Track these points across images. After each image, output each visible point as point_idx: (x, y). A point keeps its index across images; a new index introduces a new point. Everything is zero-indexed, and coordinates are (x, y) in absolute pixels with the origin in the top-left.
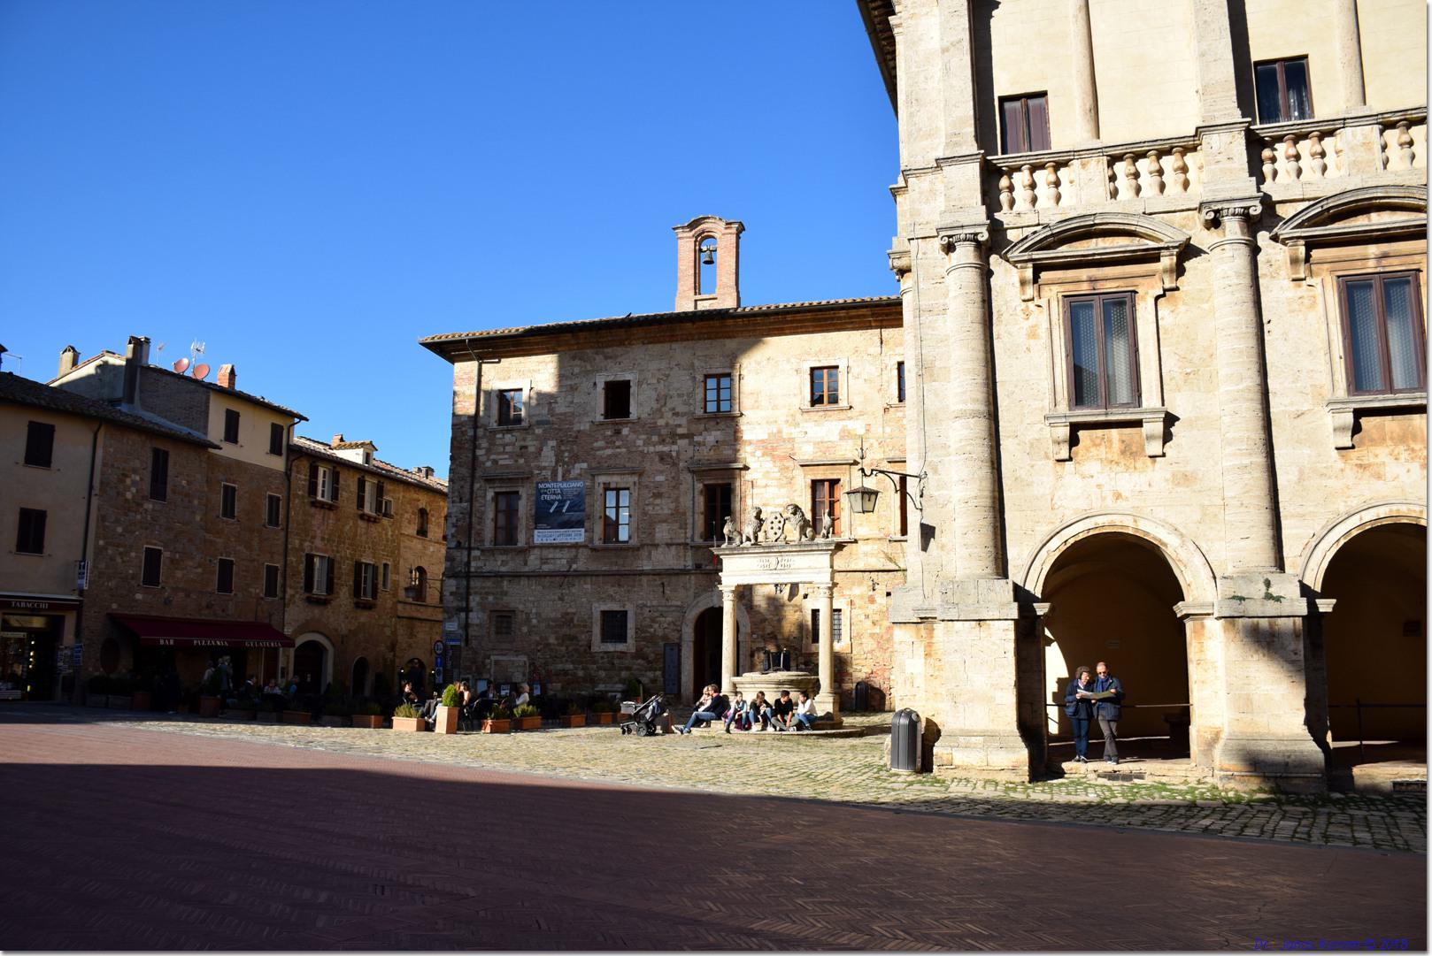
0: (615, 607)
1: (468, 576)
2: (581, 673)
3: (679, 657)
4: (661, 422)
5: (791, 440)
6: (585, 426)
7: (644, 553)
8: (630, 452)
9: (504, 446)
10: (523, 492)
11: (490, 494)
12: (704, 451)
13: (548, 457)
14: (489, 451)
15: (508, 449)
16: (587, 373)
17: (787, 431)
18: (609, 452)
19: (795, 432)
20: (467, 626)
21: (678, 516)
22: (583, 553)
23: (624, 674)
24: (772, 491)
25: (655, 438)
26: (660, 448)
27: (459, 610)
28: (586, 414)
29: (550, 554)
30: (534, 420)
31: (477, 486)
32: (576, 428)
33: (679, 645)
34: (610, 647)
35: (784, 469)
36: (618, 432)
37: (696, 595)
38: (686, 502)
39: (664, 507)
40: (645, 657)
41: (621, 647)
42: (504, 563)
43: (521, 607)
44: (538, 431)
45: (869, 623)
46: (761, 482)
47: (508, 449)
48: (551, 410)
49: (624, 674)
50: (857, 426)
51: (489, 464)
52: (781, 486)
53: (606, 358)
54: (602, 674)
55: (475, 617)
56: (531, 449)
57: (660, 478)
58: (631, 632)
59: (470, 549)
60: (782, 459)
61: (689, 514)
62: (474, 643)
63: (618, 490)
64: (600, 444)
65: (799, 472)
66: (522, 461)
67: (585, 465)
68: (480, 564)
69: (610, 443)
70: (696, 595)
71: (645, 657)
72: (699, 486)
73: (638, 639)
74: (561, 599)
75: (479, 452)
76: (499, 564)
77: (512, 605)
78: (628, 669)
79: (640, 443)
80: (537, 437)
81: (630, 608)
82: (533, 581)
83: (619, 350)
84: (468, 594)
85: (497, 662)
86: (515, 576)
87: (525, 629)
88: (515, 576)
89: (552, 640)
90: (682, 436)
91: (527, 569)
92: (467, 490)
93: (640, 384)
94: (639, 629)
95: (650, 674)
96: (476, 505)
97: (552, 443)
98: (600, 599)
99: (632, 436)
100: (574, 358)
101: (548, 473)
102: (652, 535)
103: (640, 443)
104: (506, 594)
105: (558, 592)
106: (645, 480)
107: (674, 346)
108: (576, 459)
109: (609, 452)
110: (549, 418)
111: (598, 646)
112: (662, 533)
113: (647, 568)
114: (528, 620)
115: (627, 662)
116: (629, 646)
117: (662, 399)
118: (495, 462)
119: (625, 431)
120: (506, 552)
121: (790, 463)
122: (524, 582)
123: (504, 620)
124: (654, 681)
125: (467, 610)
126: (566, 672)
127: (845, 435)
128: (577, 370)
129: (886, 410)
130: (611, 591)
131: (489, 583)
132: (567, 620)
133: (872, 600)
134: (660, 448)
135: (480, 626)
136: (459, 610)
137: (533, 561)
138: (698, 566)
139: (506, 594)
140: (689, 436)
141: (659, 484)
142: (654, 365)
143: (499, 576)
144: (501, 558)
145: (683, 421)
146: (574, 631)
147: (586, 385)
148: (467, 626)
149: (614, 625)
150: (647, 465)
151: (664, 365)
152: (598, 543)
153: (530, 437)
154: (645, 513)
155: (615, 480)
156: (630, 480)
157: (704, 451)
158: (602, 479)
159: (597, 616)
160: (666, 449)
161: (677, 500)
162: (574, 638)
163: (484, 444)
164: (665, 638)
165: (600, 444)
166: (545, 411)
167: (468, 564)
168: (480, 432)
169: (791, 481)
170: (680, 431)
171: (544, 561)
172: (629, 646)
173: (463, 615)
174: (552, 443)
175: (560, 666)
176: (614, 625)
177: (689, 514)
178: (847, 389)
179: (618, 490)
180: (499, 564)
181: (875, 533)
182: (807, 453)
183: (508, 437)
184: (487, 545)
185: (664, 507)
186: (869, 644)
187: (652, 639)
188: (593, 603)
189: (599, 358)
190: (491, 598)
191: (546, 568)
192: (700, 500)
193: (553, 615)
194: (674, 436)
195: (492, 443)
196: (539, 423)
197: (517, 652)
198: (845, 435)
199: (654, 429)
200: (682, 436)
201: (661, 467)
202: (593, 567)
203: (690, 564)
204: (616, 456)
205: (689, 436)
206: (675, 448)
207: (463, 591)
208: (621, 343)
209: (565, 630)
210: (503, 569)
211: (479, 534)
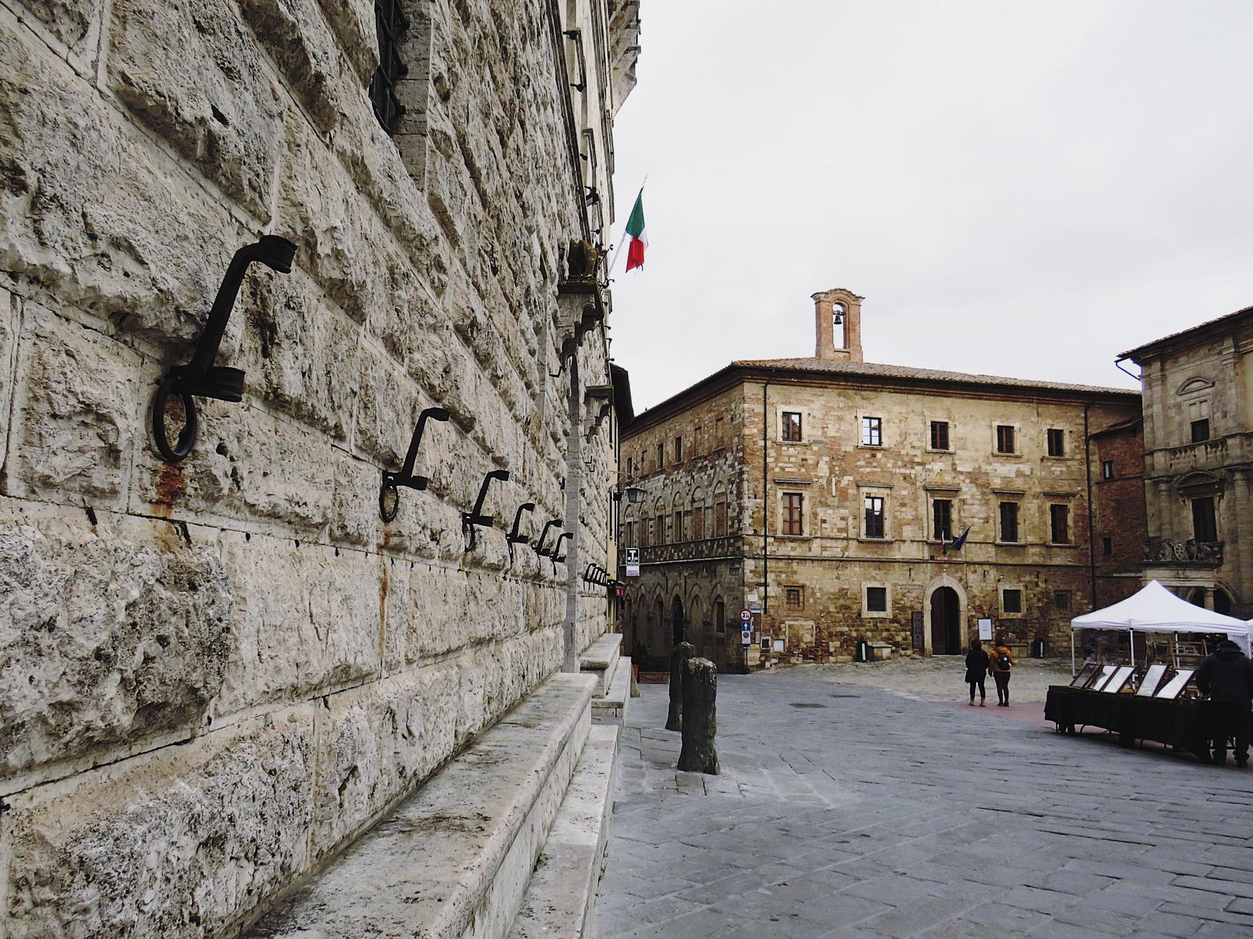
0: (878, 585)
1: (766, 558)
2: (854, 634)
3: (922, 622)
4: (903, 452)
5: (987, 474)
6: (850, 449)
7: (896, 545)
8: (883, 471)
9: (789, 457)
10: (806, 494)
11: (780, 494)
12: (933, 475)
13: (823, 470)
14: (777, 460)
15: (792, 459)
16: (850, 408)
17: (985, 468)
18: (868, 470)
19: (989, 468)
20: (766, 598)
21: (917, 519)
22: (853, 544)
23: (885, 634)
24: (975, 509)
25: (900, 463)
26: (903, 471)
27: (759, 585)
28: (850, 439)
29: (828, 543)
30: (812, 439)
31: (768, 486)
32: (843, 449)
33: (921, 614)
34: (875, 614)
35: (984, 494)
36: (874, 456)
37: (932, 578)
38: (922, 510)
39: (908, 514)
40: (899, 622)
41: (882, 614)
42: (793, 549)
43: (808, 584)
44: (815, 448)
45: (1035, 600)
46: (969, 501)
47: (792, 459)
48: (824, 434)
49: (885, 634)
50: (1026, 469)
51: (777, 470)
52: (981, 505)
53: (863, 399)
54: (869, 634)
55: (773, 590)
56: (810, 462)
57: (904, 493)
58: (889, 604)
59: (766, 536)
60: (983, 486)
61: (925, 520)
62: (772, 611)
63: (873, 498)
64: (861, 463)
65: (992, 496)
66: (803, 470)
67: (851, 478)
68: (774, 548)
69: (869, 464)
70: (932, 578)
71: (899, 622)
72: (931, 501)
73: (894, 608)
74: (838, 578)
75: (768, 460)
76: (787, 549)
77: (801, 582)
78: (888, 630)
79: (890, 465)
80: (815, 453)
81: (888, 586)
82: (815, 564)
83: (871, 394)
84: (766, 572)
85: (790, 626)
86: (802, 560)
87: (811, 601)
88: (802, 560)
89: (832, 609)
90: (918, 464)
91: (810, 554)
92: (761, 488)
93: (888, 422)
94: (895, 602)
95: (903, 634)
96: (769, 502)
97: (827, 459)
98: (865, 579)
99: (884, 460)
100: (839, 395)
101: (824, 482)
102: (900, 533)
103: (890, 465)
104: (795, 573)
105: (836, 573)
106: (894, 493)
107: (911, 397)
108: (844, 473)
109: (868, 470)
110: (823, 439)
111: (866, 614)
112: (908, 532)
113: (898, 556)
114: (813, 593)
115: (887, 625)
116: (888, 613)
117: (905, 435)
118: (783, 469)
119: (879, 455)
120: (793, 540)
121: (987, 491)
122: (809, 564)
123: (794, 593)
124: (905, 639)
125: (766, 585)
126: (842, 634)
127: (1019, 474)
128: (842, 405)
129: (1042, 460)
130: (874, 573)
131: (781, 564)
132: (843, 593)
133: (1037, 585)
134: (903, 471)
135: (776, 597)
136: (759, 585)
137: (816, 549)
138: (932, 558)
139: (795, 573)
140: (922, 464)
141: (903, 497)
142: (897, 409)
143: (790, 559)
144: (790, 545)
145: (918, 453)
146: (848, 603)
147: (849, 417)
148: (766, 598)
149: (876, 598)
150: (895, 482)
151: (904, 410)
152: (863, 537)
153: (809, 452)
154: (895, 517)
155: (874, 492)
156: (883, 493)
157: (933, 475)
158: (865, 490)
159: (865, 591)
160: (907, 472)
161: (916, 509)
162: (848, 608)
163: (771, 453)
164: (912, 608)
165: (861, 463)
166: (820, 433)
167: (765, 548)
168: (769, 443)
169: (987, 503)
170: (917, 460)
171: (824, 548)
172: (888, 613)
173: (762, 589)
174: (827, 459)
175: (839, 629)
176: (876, 598)
177: (925, 520)
178: (1019, 442)
179: (873, 498)
180: (787, 549)
181: (1037, 541)
182: (997, 483)
183: (792, 450)
184: (779, 534)
185: (908, 514)
186: (1036, 614)
187: (903, 609)
188: (860, 581)
189: (858, 398)
190: (783, 576)
191: (826, 554)
192: (932, 510)
193: (832, 590)
194: (913, 464)
195: (779, 454)
196: (815, 442)
197: (806, 619)
198: (1019, 474)
199: (899, 455)
200: (918, 464)
201: (904, 484)
202: (861, 555)
203: (927, 557)
204: (874, 473)
205: (922, 464)
206: (913, 471)
207: (761, 569)
208: (875, 390)
209: (841, 602)
210: (792, 554)
211: (772, 525)
